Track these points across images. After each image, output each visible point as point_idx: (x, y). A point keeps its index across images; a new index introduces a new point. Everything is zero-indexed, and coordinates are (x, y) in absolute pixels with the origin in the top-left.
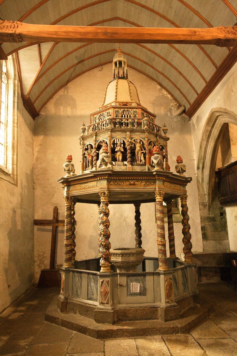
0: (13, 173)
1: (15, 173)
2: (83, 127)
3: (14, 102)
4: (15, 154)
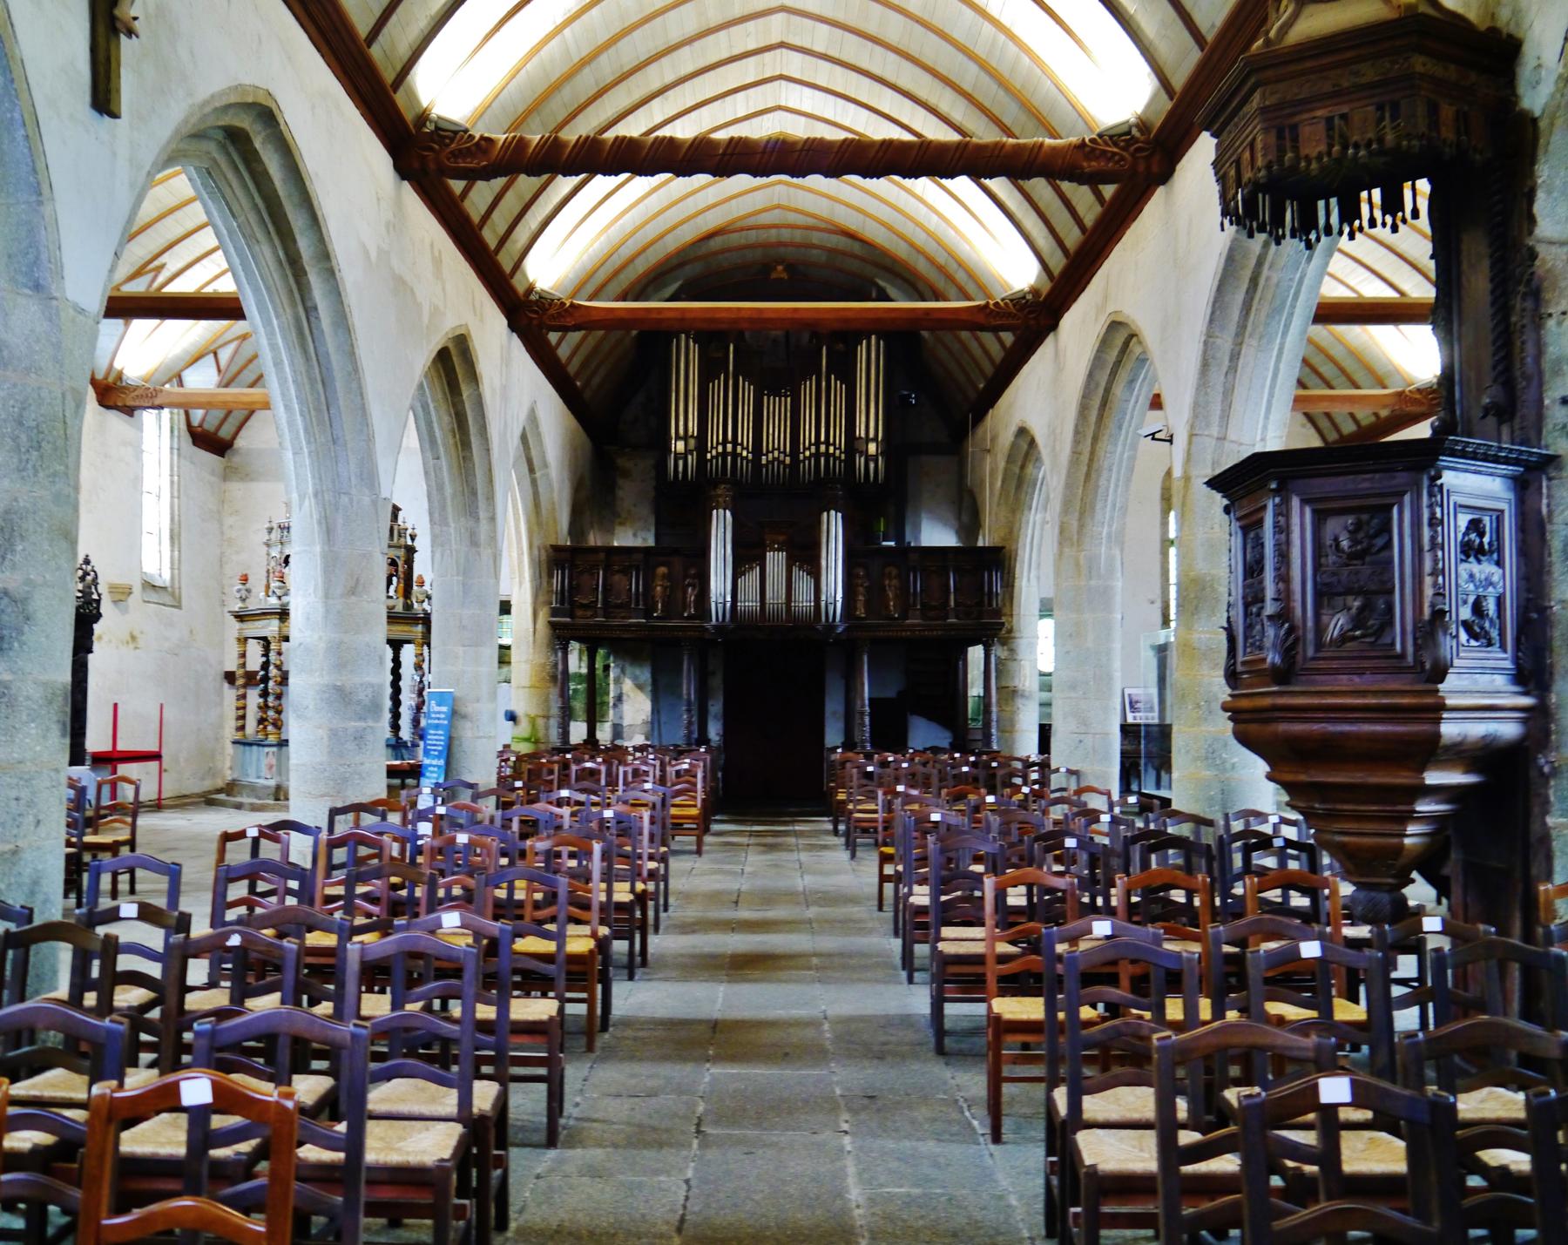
0: (172, 587)
1: (177, 585)
2: (267, 525)
3: (172, 448)
4: (176, 549)
